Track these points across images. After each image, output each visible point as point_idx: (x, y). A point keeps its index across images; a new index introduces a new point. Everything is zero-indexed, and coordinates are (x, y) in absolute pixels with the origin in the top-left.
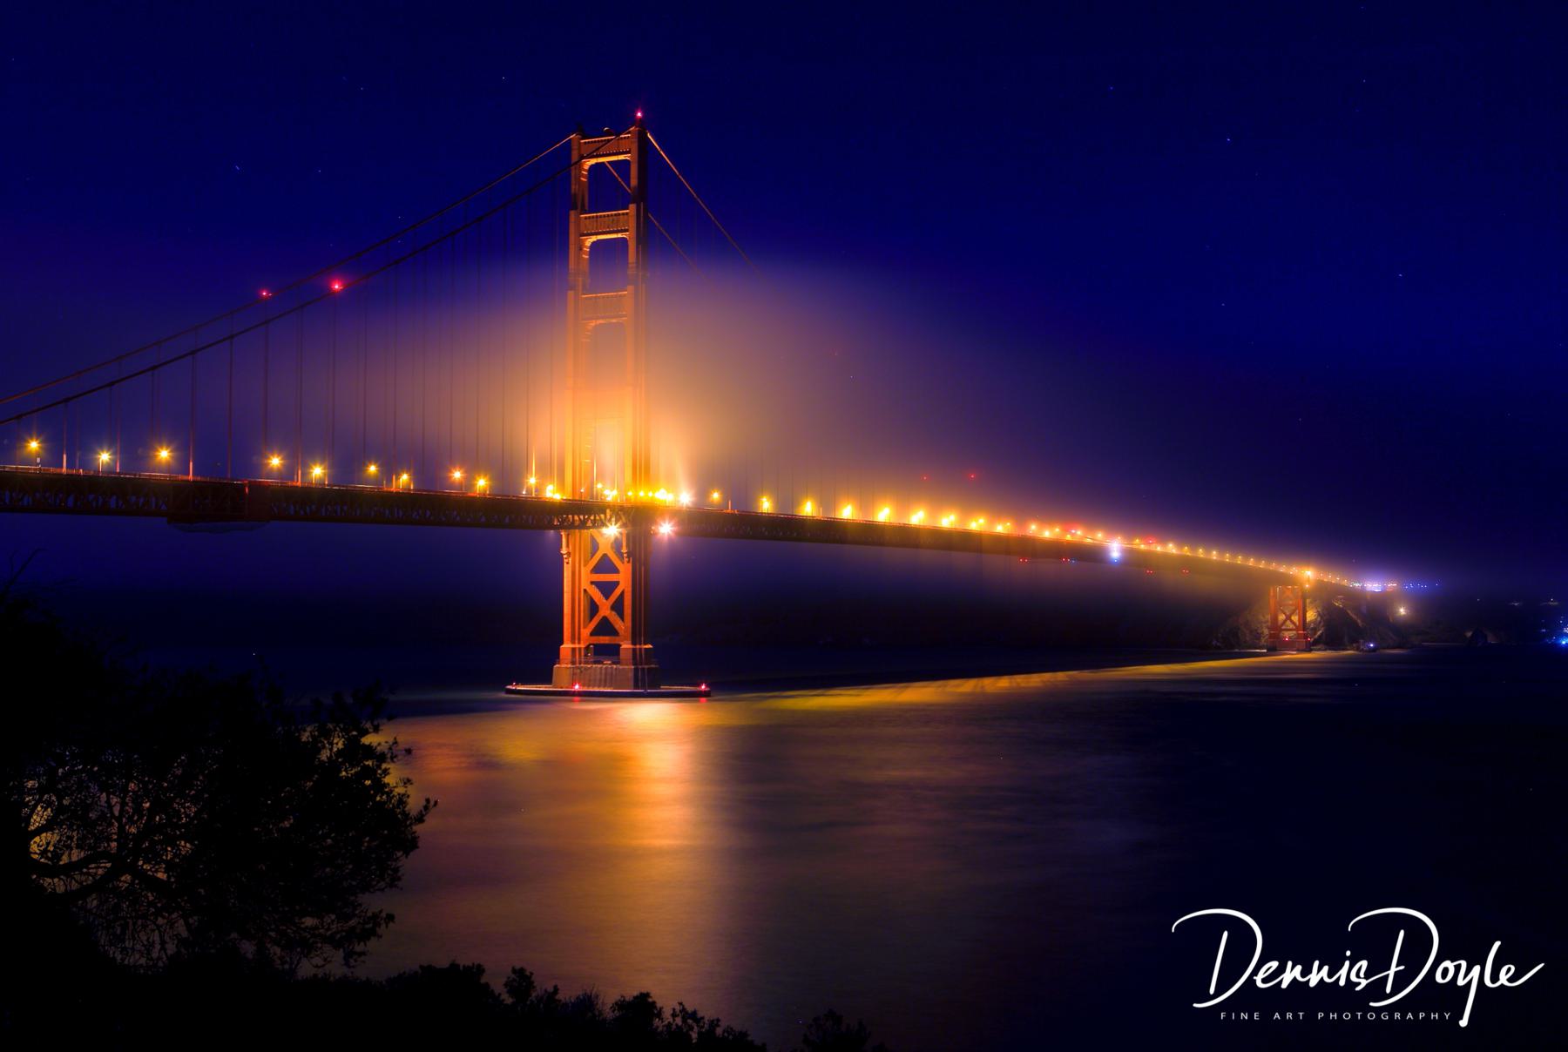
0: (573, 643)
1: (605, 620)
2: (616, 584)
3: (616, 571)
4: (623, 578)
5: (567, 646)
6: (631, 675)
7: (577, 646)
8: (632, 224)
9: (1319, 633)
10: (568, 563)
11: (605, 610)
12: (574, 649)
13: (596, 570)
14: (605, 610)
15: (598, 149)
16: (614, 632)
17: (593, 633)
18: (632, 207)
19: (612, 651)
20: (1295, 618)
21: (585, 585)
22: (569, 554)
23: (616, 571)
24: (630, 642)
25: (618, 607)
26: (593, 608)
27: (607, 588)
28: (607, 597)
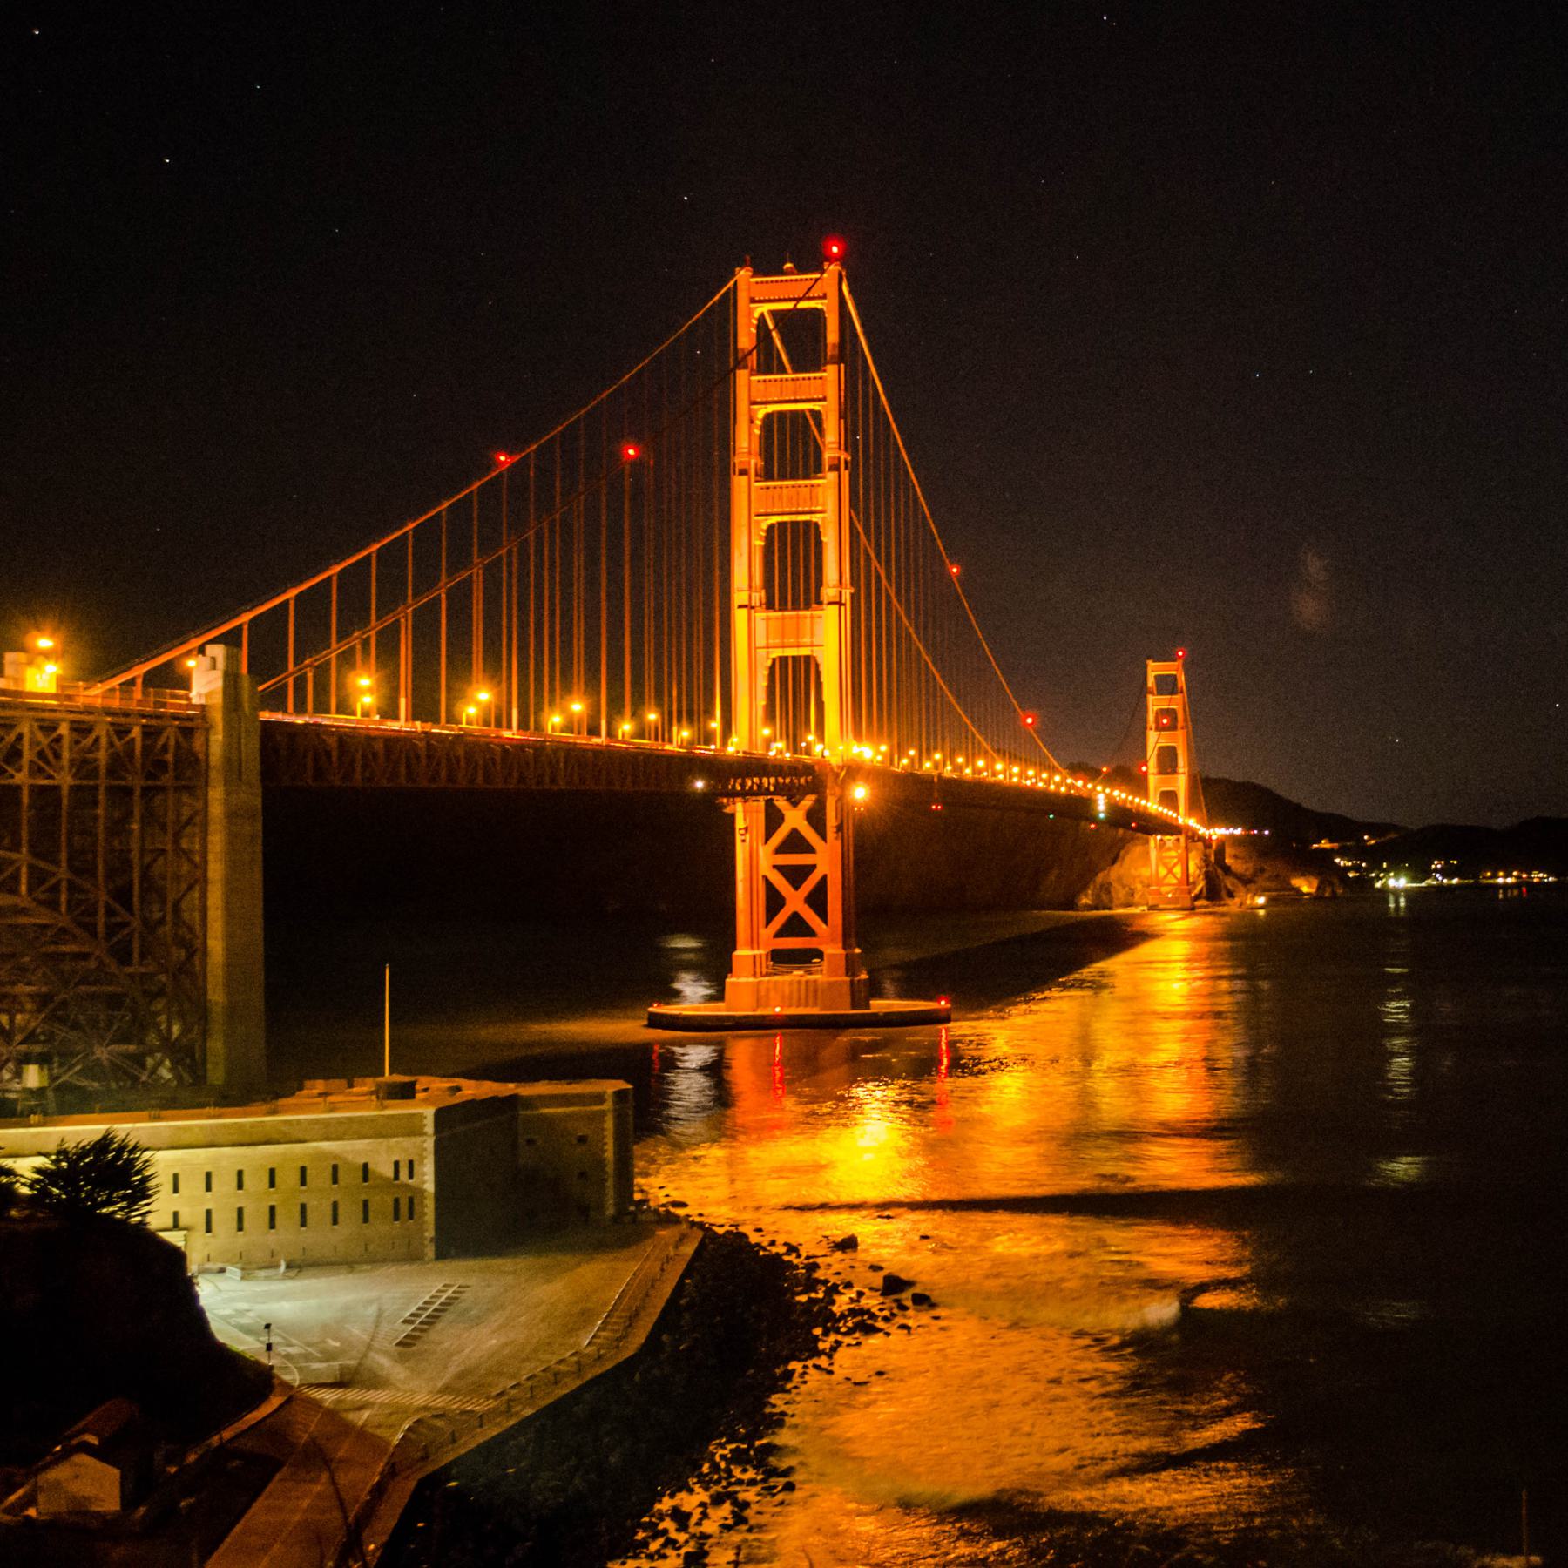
0: (752, 948)
1: (796, 917)
2: (813, 867)
3: (810, 849)
4: (826, 860)
5: (742, 953)
6: (846, 990)
7: (756, 952)
8: (832, 392)
9: (1198, 888)
10: (744, 841)
11: (795, 901)
12: (754, 956)
13: (780, 850)
14: (795, 901)
15: (809, 290)
16: (809, 932)
17: (780, 934)
18: (831, 373)
19: (805, 958)
20: (1178, 870)
21: (765, 866)
22: (746, 829)
23: (810, 849)
24: (841, 945)
25: (817, 900)
26: (774, 901)
27: (796, 875)
28: (796, 885)
